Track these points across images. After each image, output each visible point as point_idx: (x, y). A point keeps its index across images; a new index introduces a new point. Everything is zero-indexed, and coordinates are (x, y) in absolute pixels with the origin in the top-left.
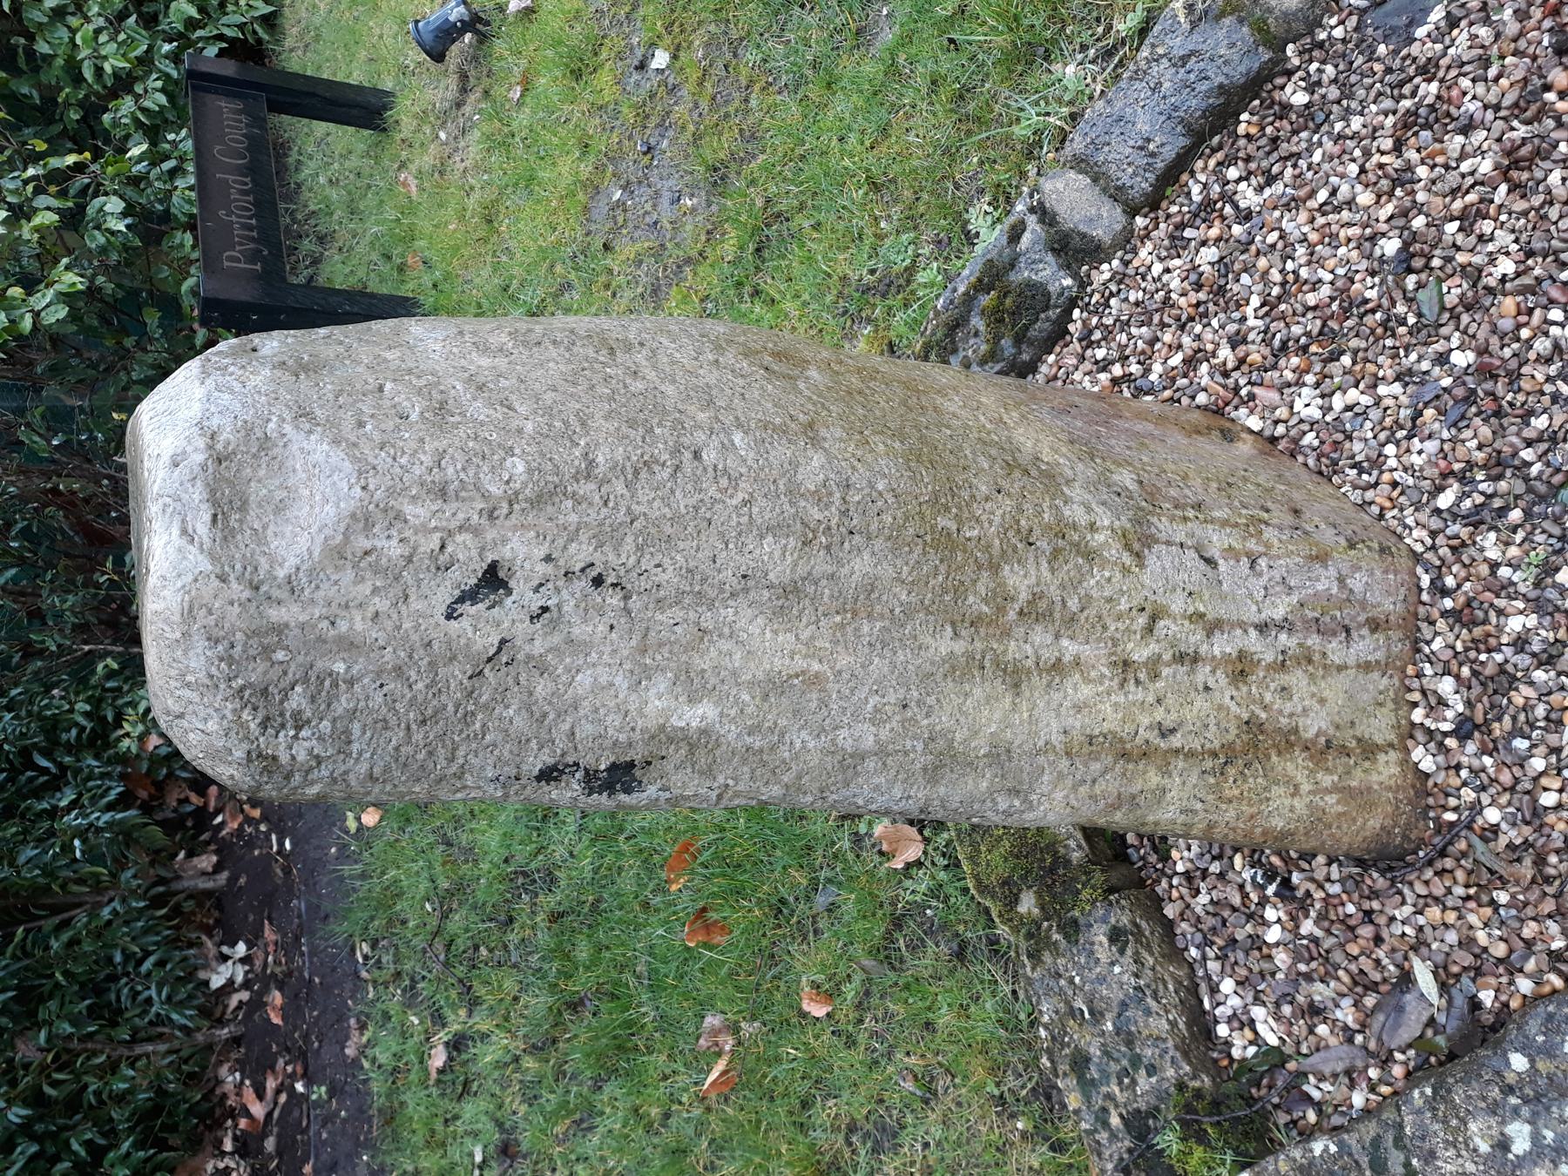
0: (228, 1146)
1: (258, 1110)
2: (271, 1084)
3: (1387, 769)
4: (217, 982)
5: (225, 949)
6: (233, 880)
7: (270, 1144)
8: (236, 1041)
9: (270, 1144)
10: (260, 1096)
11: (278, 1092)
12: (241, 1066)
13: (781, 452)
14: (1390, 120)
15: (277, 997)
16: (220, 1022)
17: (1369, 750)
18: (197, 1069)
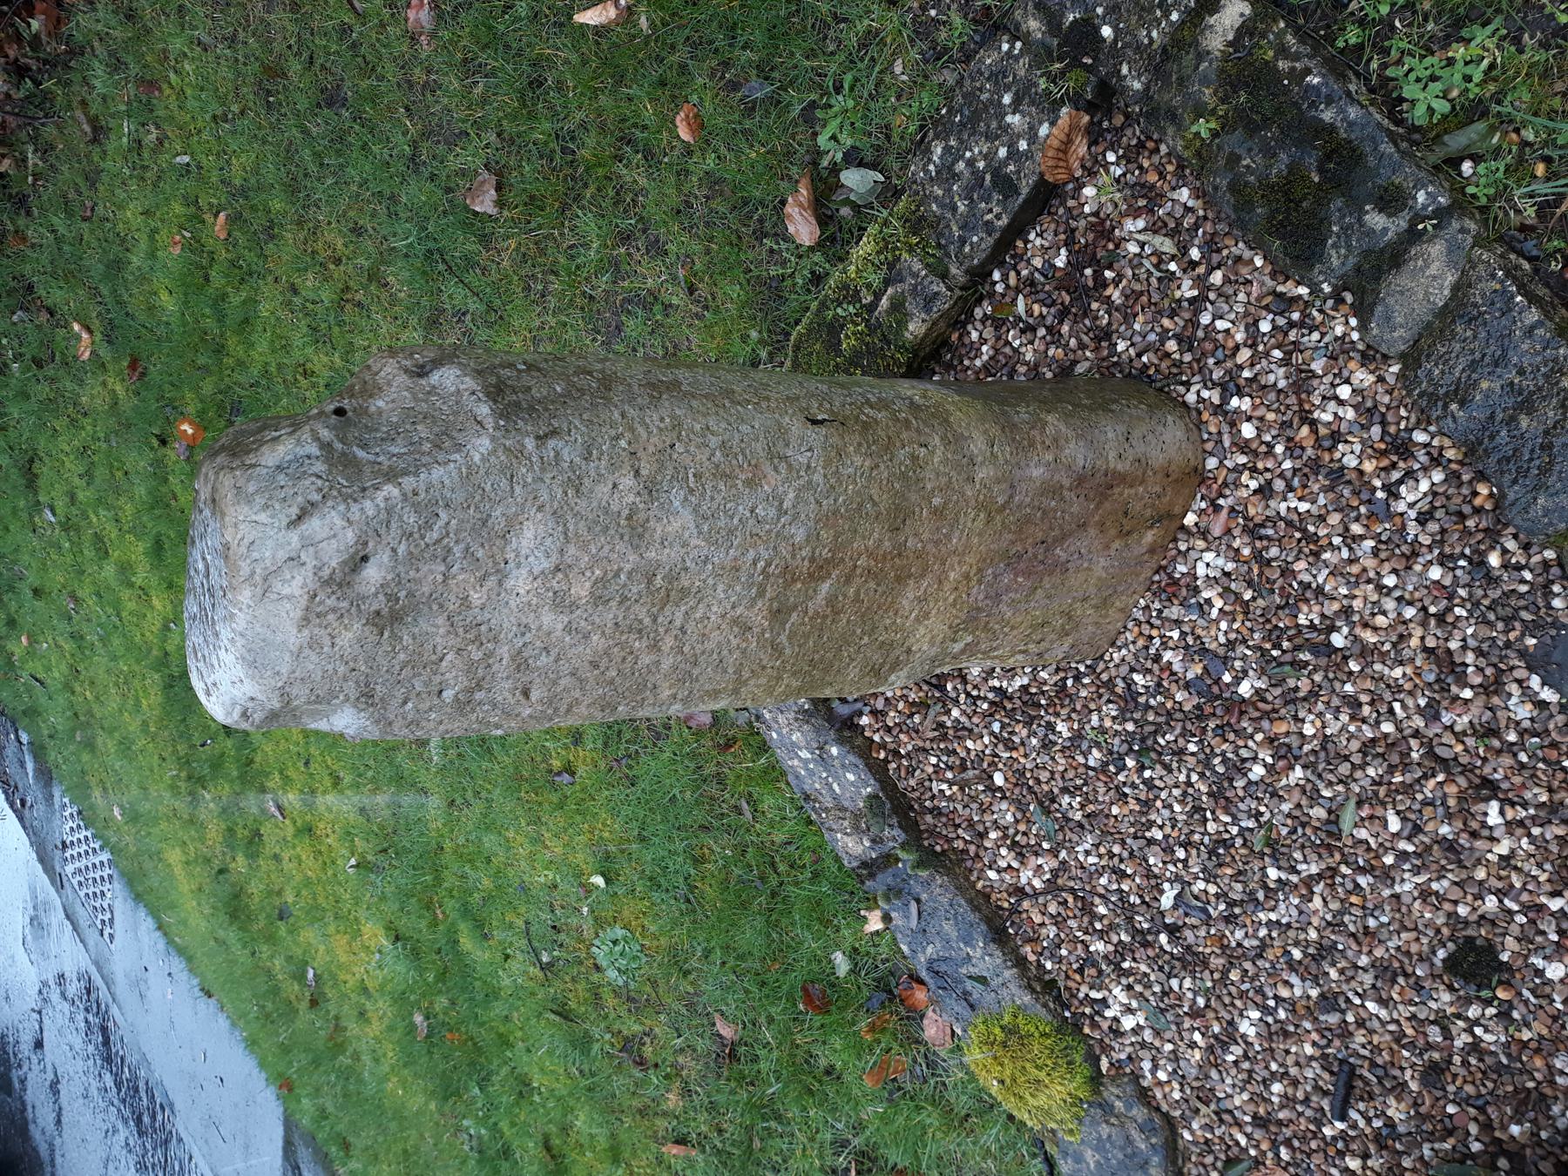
14: (1454, 645)
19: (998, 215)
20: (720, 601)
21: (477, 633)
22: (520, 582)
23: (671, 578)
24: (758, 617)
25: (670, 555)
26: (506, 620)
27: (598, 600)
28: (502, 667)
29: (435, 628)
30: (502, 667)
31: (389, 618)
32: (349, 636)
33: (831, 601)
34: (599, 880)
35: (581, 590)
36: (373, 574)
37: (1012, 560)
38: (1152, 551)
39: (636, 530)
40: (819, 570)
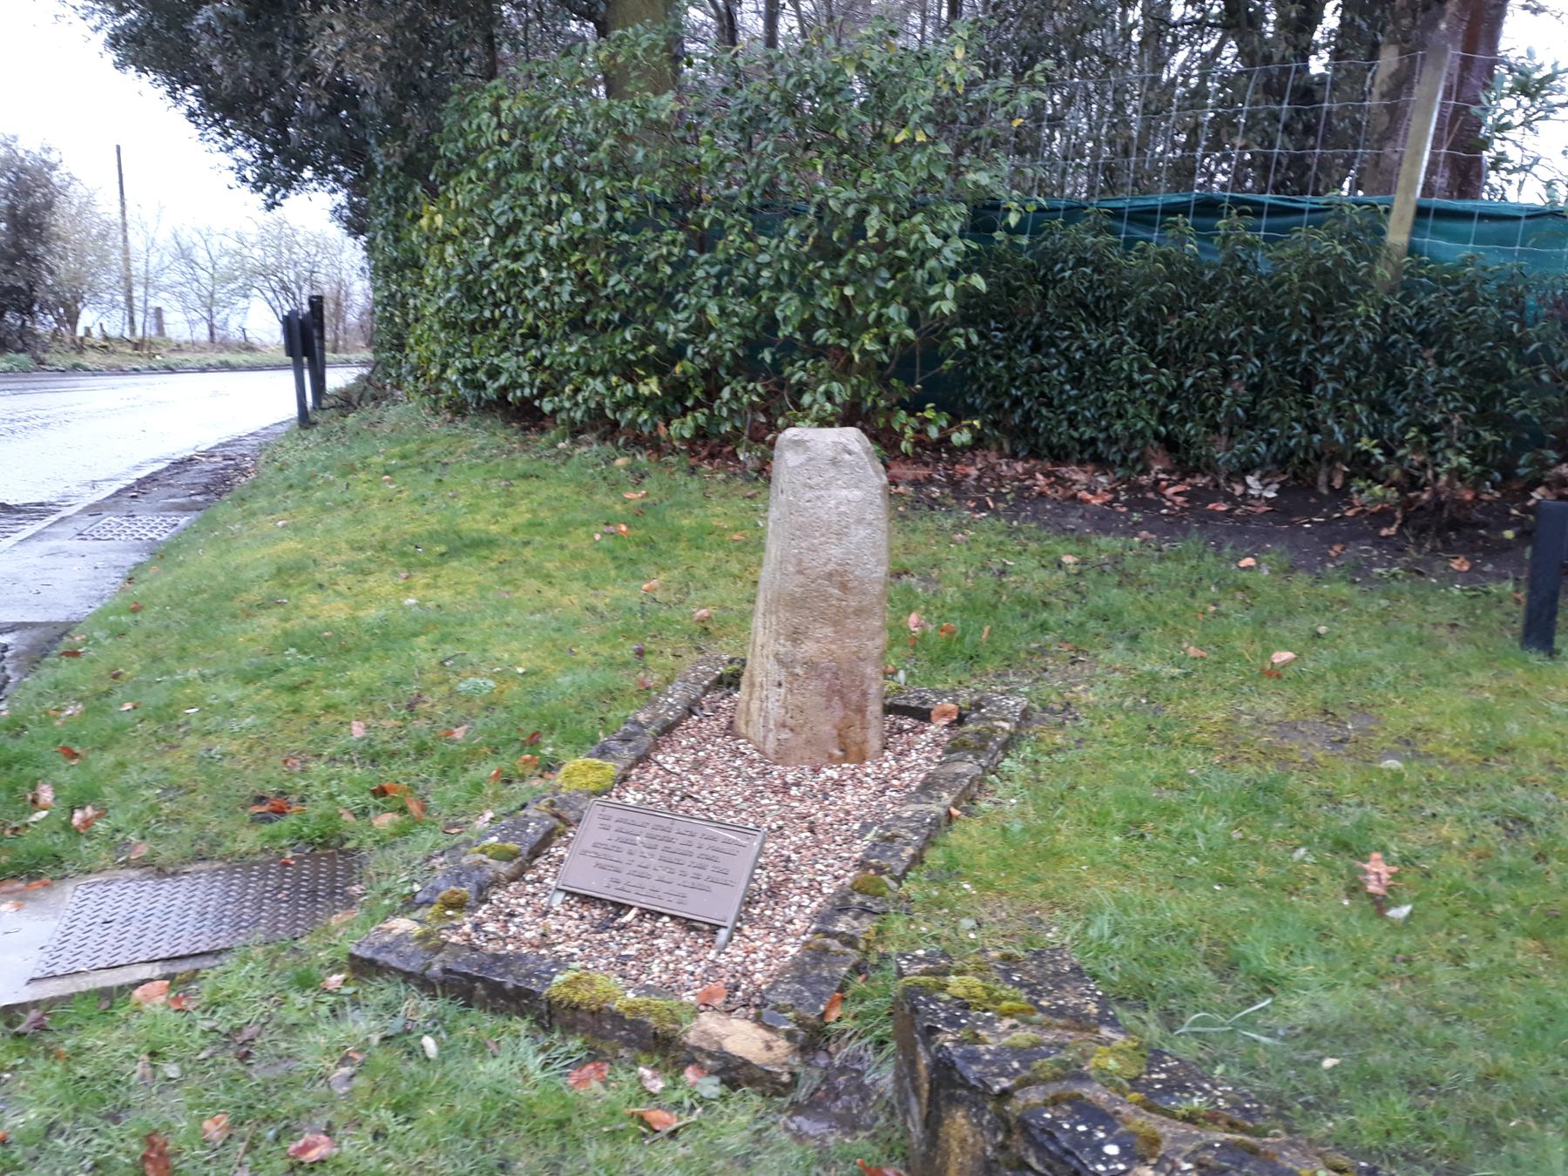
0: (1161, 476)
1: (1171, 491)
2: (1179, 499)
3: (743, 730)
4: (1250, 480)
5: (1276, 486)
6: (1319, 496)
7: (1151, 495)
8: (1217, 486)
9: (1151, 495)
10: (1177, 494)
11: (1174, 502)
12: (1205, 487)
13: (793, 561)
15: (1223, 507)
16: (1228, 480)
17: (747, 723)
18: (1208, 467)
19: (914, 703)
20: (836, 552)
21: (828, 485)
22: (844, 493)
23: (846, 534)
24: (830, 567)
25: (853, 532)
26: (834, 491)
27: (839, 514)
28: (818, 493)
29: (832, 473)
30: (818, 493)
31: (834, 462)
32: (830, 454)
33: (831, 596)
34: (521, 670)
35: (843, 508)
36: (847, 457)
37: (836, 676)
38: (831, 756)
39: (860, 521)
40: (844, 587)
